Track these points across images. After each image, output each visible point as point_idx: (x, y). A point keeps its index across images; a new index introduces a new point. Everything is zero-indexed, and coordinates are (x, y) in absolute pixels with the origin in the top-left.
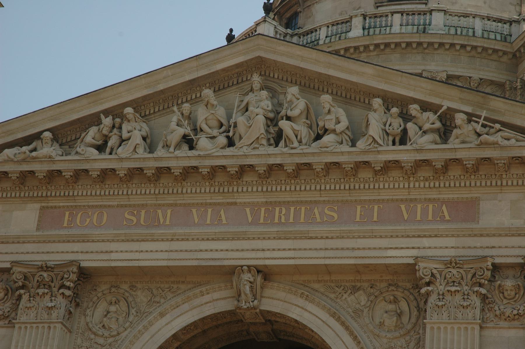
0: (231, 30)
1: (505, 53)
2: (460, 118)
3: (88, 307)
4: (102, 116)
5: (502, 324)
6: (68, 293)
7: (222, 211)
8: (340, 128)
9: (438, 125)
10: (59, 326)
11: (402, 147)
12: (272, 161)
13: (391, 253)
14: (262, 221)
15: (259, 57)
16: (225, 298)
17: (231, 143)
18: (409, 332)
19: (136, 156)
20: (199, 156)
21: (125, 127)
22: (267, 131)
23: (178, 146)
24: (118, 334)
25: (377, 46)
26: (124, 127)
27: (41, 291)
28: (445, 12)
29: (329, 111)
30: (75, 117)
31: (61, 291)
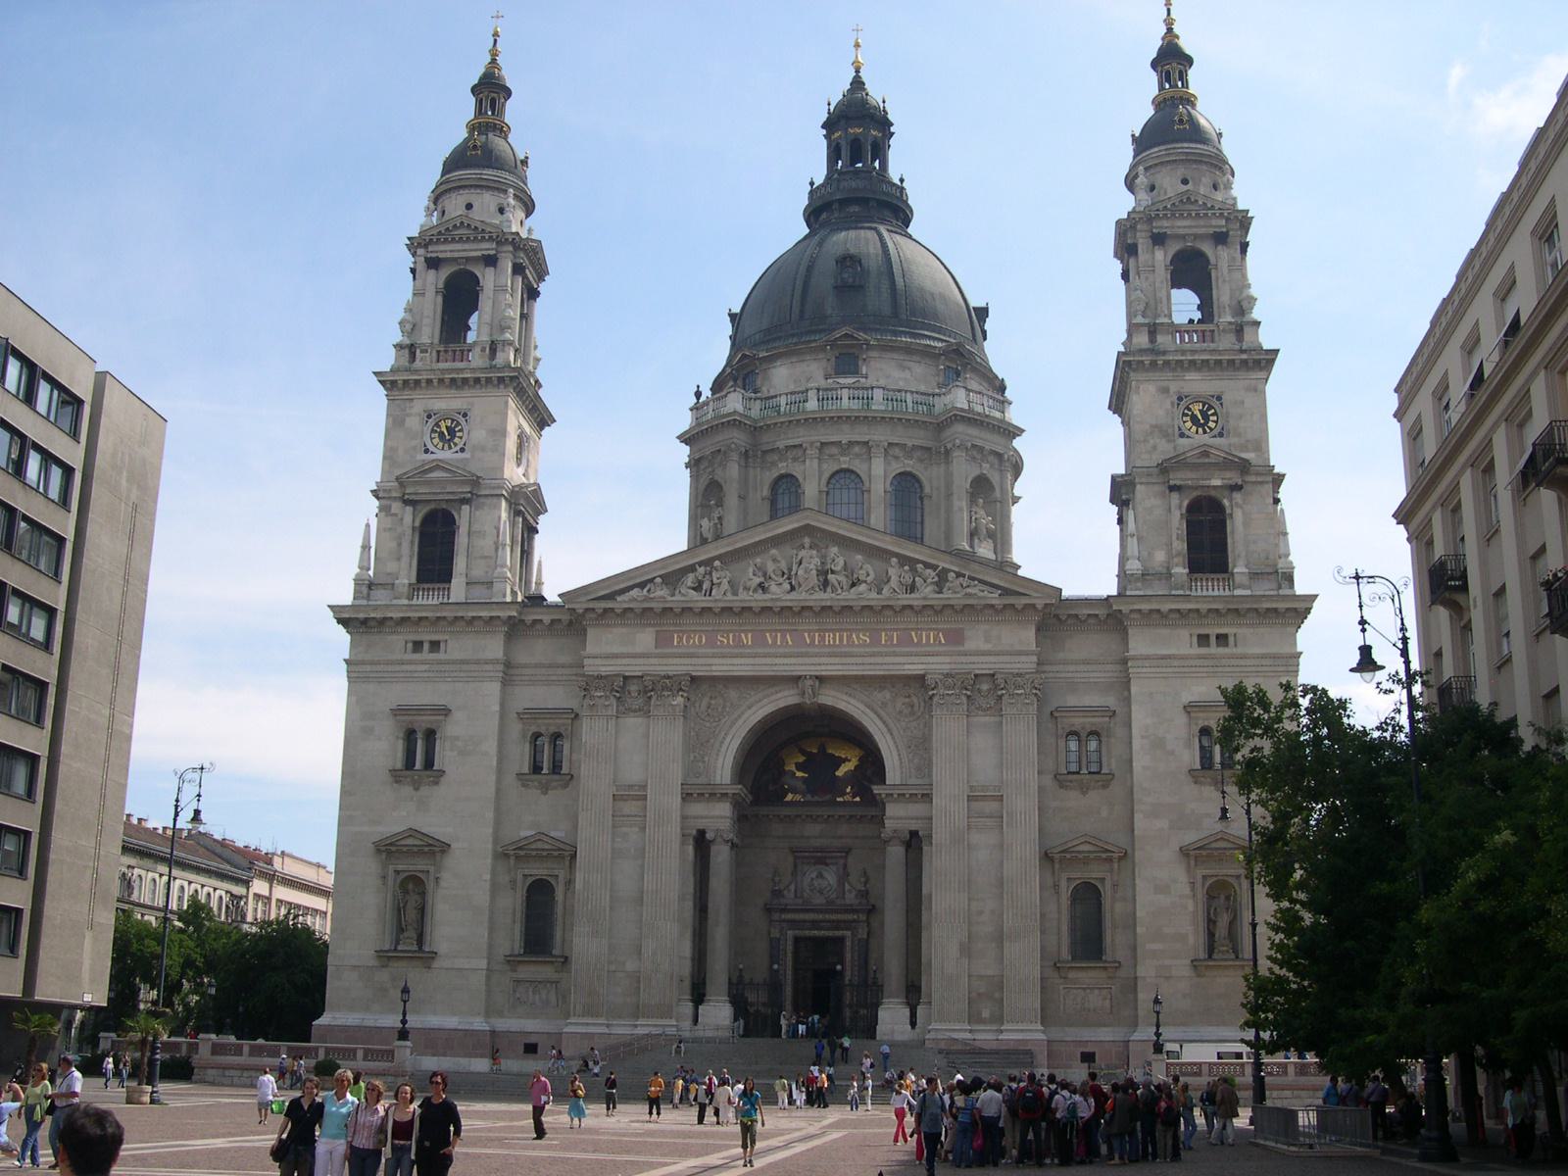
0: (698, 387)
1: (931, 423)
3: (695, 701)
4: (697, 567)
5: (980, 712)
6: (685, 695)
7: (788, 637)
8: (869, 579)
9: (936, 579)
10: (682, 718)
11: (913, 595)
12: (824, 604)
13: (907, 667)
14: (817, 643)
15: (808, 525)
16: (793, 695)
17: (793, 588)
18: (919, 717)
19: (726, 598)
20: (772, 599)
21: (715, 575)
22: (819, 580)
23: (755, 591)
24: (720, 720)
25: (832, 418)
26: (713, 574)
27: (666, 693)
28: (884, 389)
29: (861, 568)
30: (678, 567)
31: (680, 693)
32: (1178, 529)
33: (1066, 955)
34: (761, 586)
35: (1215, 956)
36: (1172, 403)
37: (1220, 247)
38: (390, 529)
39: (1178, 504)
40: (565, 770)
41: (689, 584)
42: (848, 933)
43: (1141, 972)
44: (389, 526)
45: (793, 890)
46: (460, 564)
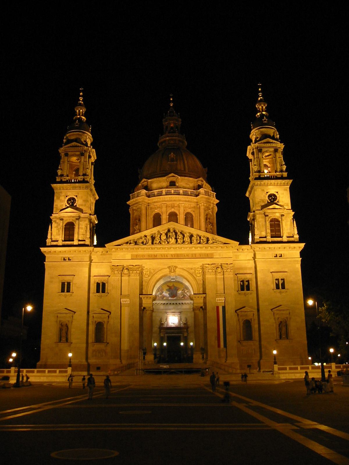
2: (210, 240)
21: (147, 239)
32: (268, 226)
33: (242, 339)
34: (160, 242)
35: (282, 339)
36: (265, 194)
37: (276, 153)
38: (56, 227)
39: (268, 220)
40: (106, 292)
41: (141, 242)
42: (182, 335)
43: (262, 343)
44: (56, 226)
45: (166, 324)
46: (76, 237)
